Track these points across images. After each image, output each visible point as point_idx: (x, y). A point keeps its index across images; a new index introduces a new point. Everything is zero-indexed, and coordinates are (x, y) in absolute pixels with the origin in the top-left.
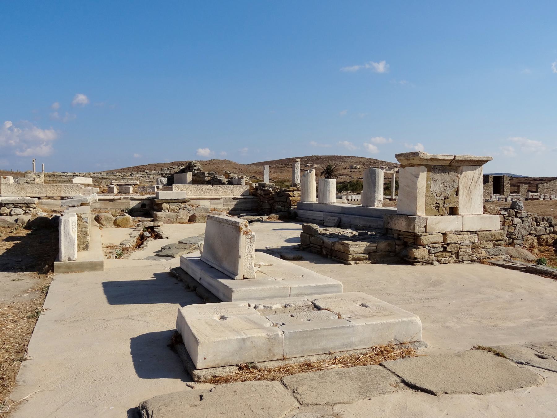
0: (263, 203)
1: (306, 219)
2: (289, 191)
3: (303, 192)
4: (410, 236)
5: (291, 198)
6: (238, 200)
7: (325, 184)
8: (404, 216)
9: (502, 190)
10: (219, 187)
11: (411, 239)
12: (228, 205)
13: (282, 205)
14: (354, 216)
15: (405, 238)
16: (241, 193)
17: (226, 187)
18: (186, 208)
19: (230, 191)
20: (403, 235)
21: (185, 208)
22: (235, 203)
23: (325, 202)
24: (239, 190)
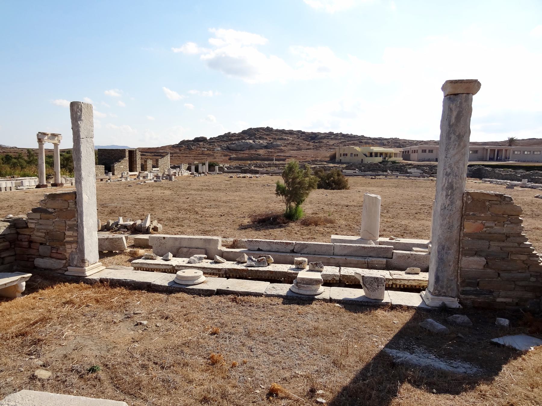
9: (135, 166)
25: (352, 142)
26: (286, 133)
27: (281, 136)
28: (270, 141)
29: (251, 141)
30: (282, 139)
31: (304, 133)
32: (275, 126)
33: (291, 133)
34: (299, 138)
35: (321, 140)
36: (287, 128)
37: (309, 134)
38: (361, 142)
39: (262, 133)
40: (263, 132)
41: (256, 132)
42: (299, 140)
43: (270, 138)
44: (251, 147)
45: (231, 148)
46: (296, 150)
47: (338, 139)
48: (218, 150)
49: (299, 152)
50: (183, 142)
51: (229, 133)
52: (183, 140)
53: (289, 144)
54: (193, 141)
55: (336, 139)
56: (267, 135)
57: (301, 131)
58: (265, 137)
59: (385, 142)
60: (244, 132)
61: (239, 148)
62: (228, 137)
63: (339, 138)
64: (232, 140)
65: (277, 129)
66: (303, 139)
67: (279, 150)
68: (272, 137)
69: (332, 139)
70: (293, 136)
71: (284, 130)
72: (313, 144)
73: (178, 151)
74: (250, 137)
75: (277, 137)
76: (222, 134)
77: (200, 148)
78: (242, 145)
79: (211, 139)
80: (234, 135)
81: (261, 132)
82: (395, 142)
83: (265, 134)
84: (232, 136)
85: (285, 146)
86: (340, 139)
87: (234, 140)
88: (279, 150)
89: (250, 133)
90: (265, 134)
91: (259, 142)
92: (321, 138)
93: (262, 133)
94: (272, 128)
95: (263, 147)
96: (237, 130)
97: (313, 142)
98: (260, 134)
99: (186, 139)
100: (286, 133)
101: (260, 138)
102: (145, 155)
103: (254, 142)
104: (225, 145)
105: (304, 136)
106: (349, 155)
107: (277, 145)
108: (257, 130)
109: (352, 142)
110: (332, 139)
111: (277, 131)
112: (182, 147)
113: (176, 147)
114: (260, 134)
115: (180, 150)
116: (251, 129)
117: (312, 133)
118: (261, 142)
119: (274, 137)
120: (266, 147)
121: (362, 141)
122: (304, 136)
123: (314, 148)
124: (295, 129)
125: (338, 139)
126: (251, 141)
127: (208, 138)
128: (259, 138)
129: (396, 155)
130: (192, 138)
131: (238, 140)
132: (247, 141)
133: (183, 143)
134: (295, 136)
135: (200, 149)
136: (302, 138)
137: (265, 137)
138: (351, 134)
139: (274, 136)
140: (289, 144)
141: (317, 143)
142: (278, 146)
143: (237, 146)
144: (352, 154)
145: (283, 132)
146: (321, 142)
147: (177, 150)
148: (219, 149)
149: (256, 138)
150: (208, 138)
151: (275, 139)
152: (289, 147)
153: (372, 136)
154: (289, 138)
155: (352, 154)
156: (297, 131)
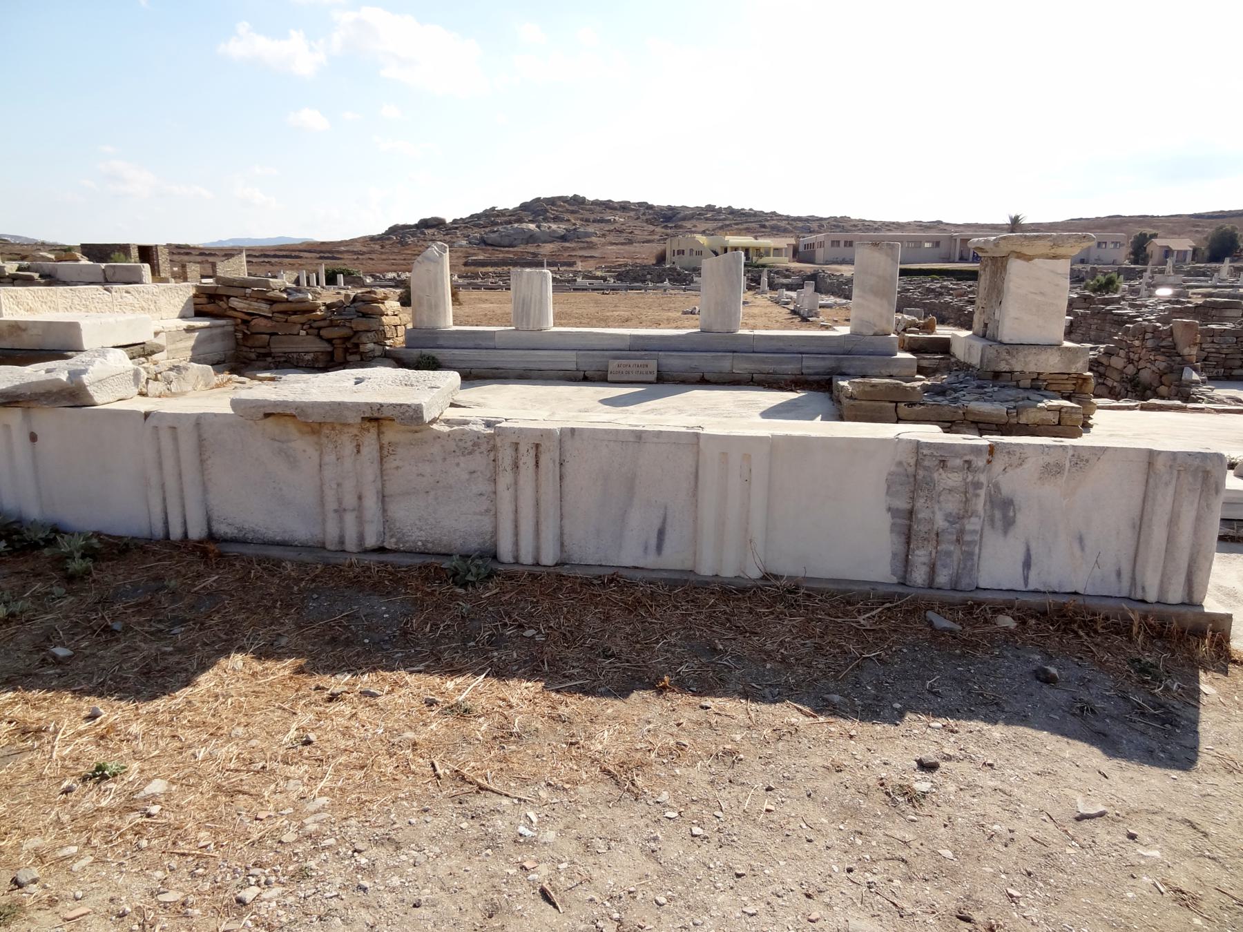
0: (273, 337)
1: (494, 371)
2: (376, 301)
3: (433, 304)
4: (1067, 379)
5: (384, 319)
6: (197, 334)
7: (544, 283)
8: (1056, 347)
10: (127, 292)
11: (1068, 386)
12: (177, 350)
13: (375, 340)
14: (713, 354)
15: (1049, 384)
16: (177, 312)
17: (142, 294)
18: (160, 373)
19: (152, 307)
20: (1045, 381)
21: (159, 376)
22: (192, 343)
23: (544, 327)
24: (172, 302)
25: (745, 226)
26: (615, 209)
27: (602, 215)
28: (575, 224)
29: (532, 226)
30: (602, 221)
31: (651, 207)
32: (592, 194)
33: (624, 207)
34: (637, 219)
35: (680, 223)
36: (617, 198)
37: (661, 208)
38: (764, 226)
39: (560, 209)
40: (565, 206)
41: (548, 207)
42: (638, 223)
43: (576, 219)
44: (531, 238)
45: (490, 242)
46: (622, 244)
47: (720, 220)
48: (461, 246)
49: (626, 247)
50: (394, 230)
51: (493, 209)
52: (395, 226)
53: (612, 231)
54: (416, 226)
55: (716, 220)
56: (573, 212)
57: (646, 203)
58: (566, 216)
59: (814, 226)
60: (524, 207)
61: (506, 241)
62: (490, 218)
63: (721, 218)
64: (497, 224)
65: (597, 200)
66: (647, 221)
67: (585, 245)
68: (581, 216)
69: (707, 219)
70: (628, 214)
71: (610, 201)
72: (663, 230)
73: (377, 247)
74: (534, 217)
75: (592, 217)
76: (479, 210)
77: (425, 240)
78: (513, 234)
79: (455, 221)
80: (503, 213)
81: (560, 206)
82: (834, 226)
83: (568, 211)
84: (498, 216)
85: (604, 235)
86: (725, 219)
87: (501, 224)
88: (585, 245)
89: (536, 209)
90: (568, 211)
91: (550, 227)
92: (684, 219)
93: (560, 209)
94: (584, 198)
95: (557, 238)
96: (510, 202)
97: (663, 227)
98: (557, 211)
99: (401, 223)
100: (615, 209)
101: (556, 219)
102: (301, 257)
103: (538, 227)
104: (476, 234)
105: (650, 214)
106: (687, 252)
107: (586, 233)
108: (552, 201)
109: (745, 226)
110: (707, 219)
111: (597, 203)
112: (389, 239)
113: (378, 239)
114: (557, 211)
115: (383, 247)
116: (538, 199)
117: (670, 208)
118: (554, 226)
119: (585, 217)
120: (563, 238)
121: (767, 224)
122: (650, 214)
123: (659, 240)
124: (634, 199)
125: (720, 220)
126: (532, 226)
127: (449, 220)
128: (554, 219)
129: (777, 251)
130: (413, 221)
131: (510, 222)
132: (524, 226)
133: (395, 231)
134: (632, 214)
135: (424, 243)
136: (644, 218)
137: (566, 216)
138: (751, 209)
139: (587, 215)
140: (612, 231)
141: (671, 228)
142: (587, 235)
143: (502, 236)
144: (691, 250)
145: (608, 205)
146: (681, 227)
147: (377, 246)
148: (464, 243)
149: (546, 220)
150: (449, 220)
151: (587, 220)
152: (611, 238)
153: (794, 213)
154: (617, 218)
155: (691, 250)
156: (638, 203)
